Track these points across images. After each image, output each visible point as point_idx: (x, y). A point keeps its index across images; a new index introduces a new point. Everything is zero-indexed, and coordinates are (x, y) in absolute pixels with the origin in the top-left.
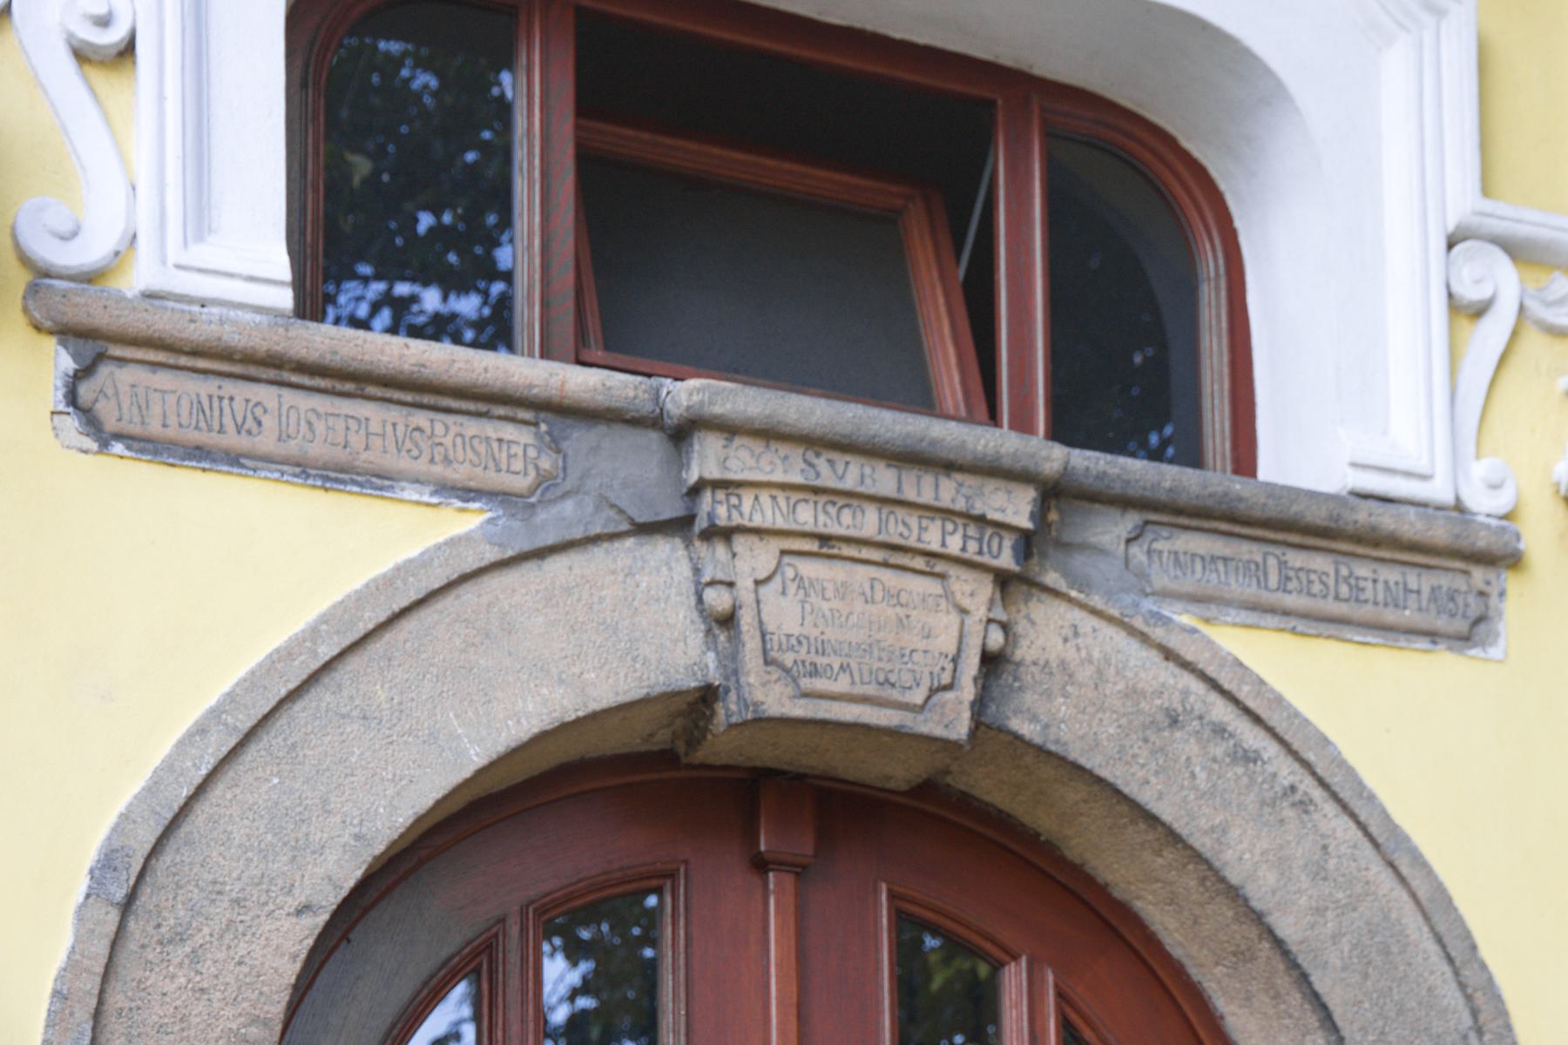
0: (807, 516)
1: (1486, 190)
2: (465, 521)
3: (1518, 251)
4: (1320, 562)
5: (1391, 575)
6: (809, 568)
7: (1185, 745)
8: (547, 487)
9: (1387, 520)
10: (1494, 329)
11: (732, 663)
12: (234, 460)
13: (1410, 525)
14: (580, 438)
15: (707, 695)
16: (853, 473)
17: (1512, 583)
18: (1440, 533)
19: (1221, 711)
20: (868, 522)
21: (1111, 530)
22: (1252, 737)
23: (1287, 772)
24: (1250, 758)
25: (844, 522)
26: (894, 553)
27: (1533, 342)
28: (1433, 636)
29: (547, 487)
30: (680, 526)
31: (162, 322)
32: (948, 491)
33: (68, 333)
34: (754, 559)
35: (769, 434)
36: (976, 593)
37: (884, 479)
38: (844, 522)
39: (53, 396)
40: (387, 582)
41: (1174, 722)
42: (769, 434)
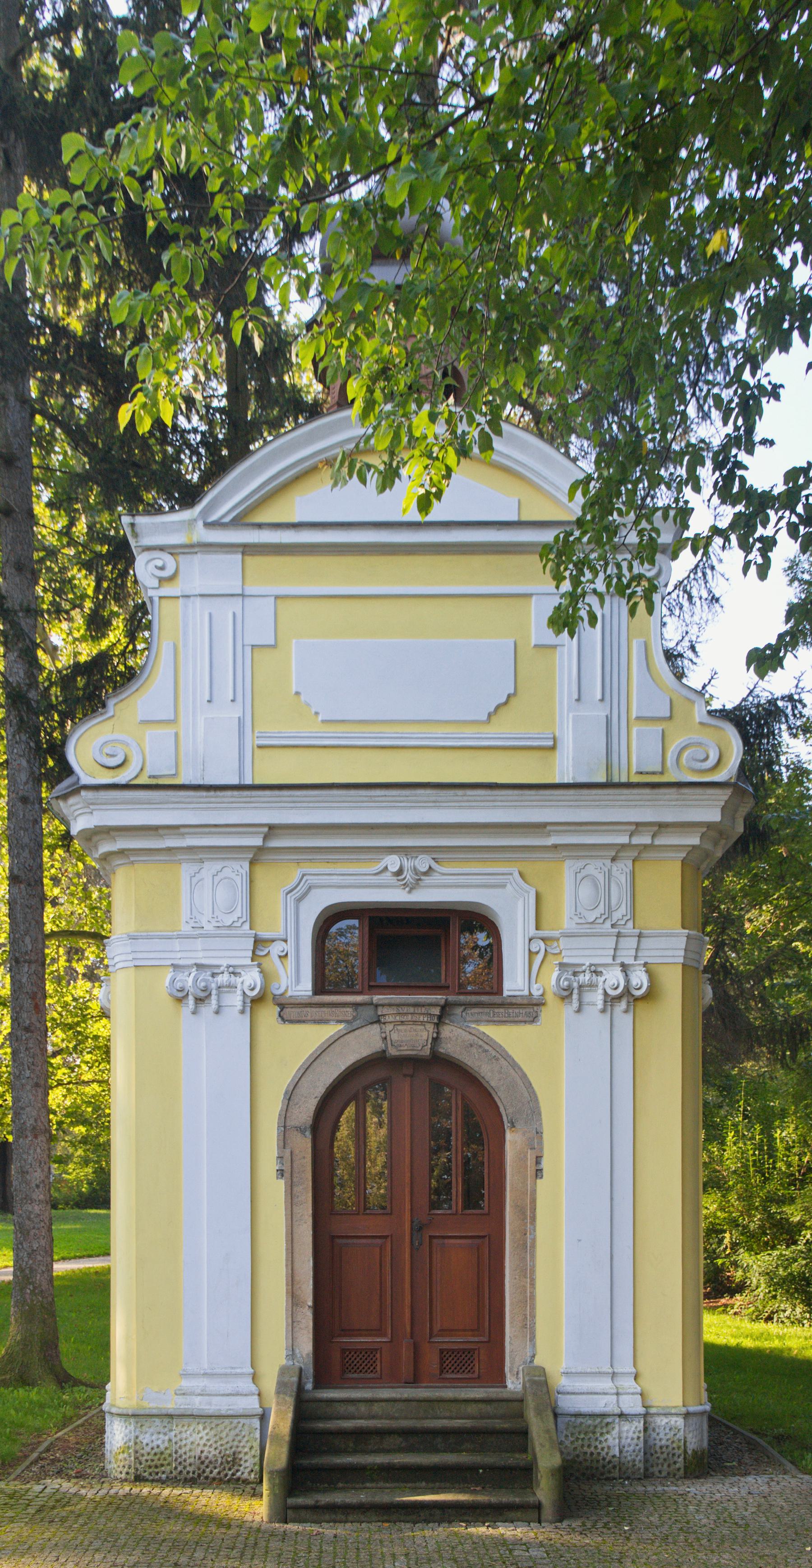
0: (398, 1018)
1: (537, 929)
2: (341, 1026)
3: (543, 939)
4: (502, 1010)
5: (517, 1011)
6: (399, 1027)
7: (474, 1050)
8: (355, 1019)
9: (514, 1001)
10: (540, 957)
11: (386, 1045)
12: (304, 1022)
13: (519, 1001)
14: (360, 1008)
15: (384, 1051)
16: (406, 1010)
17: (543, 1008)
18: (525, 1002)
19: (481, 1043)
20: (409, 1017)
21: (458, 1011)
22: (487, 1047)
23: (494, 1053)
24: (486, 1051)
25: (405, 1018)
26: (415, 1022)
27: (550, 957)
28: (525, 1022)
29: (355, 1019)
30: (378, 1021)
31: (292, 1001)
32: (423, 1010)
33: (280, 1005)
34: (389, 1027)
35: (390, 1005)
36: (431, 1028)
37: (411, 1010)
38: (405, 1018)
39: (277, 1015)
40: (328, 1040)
41: (471, 1046)
42: (390, 1005)
